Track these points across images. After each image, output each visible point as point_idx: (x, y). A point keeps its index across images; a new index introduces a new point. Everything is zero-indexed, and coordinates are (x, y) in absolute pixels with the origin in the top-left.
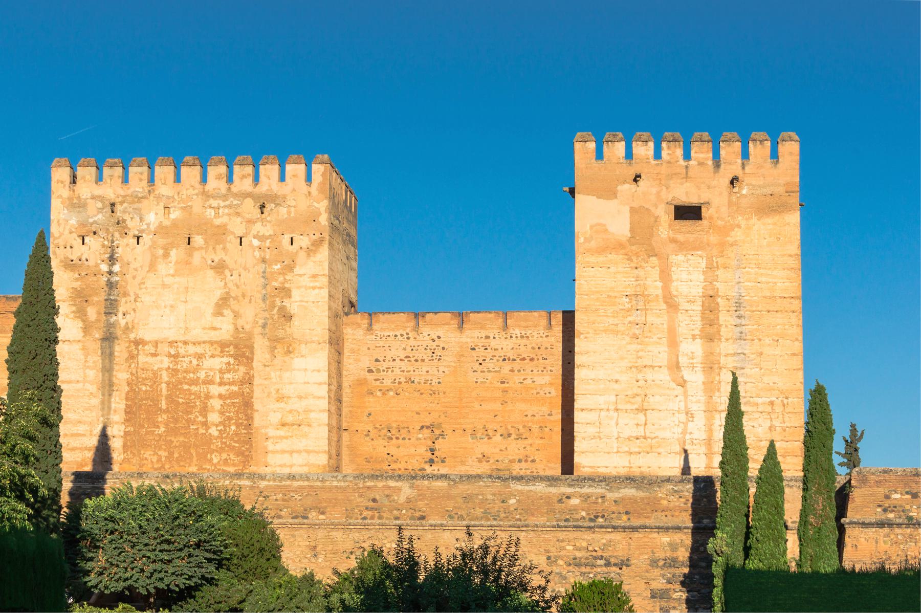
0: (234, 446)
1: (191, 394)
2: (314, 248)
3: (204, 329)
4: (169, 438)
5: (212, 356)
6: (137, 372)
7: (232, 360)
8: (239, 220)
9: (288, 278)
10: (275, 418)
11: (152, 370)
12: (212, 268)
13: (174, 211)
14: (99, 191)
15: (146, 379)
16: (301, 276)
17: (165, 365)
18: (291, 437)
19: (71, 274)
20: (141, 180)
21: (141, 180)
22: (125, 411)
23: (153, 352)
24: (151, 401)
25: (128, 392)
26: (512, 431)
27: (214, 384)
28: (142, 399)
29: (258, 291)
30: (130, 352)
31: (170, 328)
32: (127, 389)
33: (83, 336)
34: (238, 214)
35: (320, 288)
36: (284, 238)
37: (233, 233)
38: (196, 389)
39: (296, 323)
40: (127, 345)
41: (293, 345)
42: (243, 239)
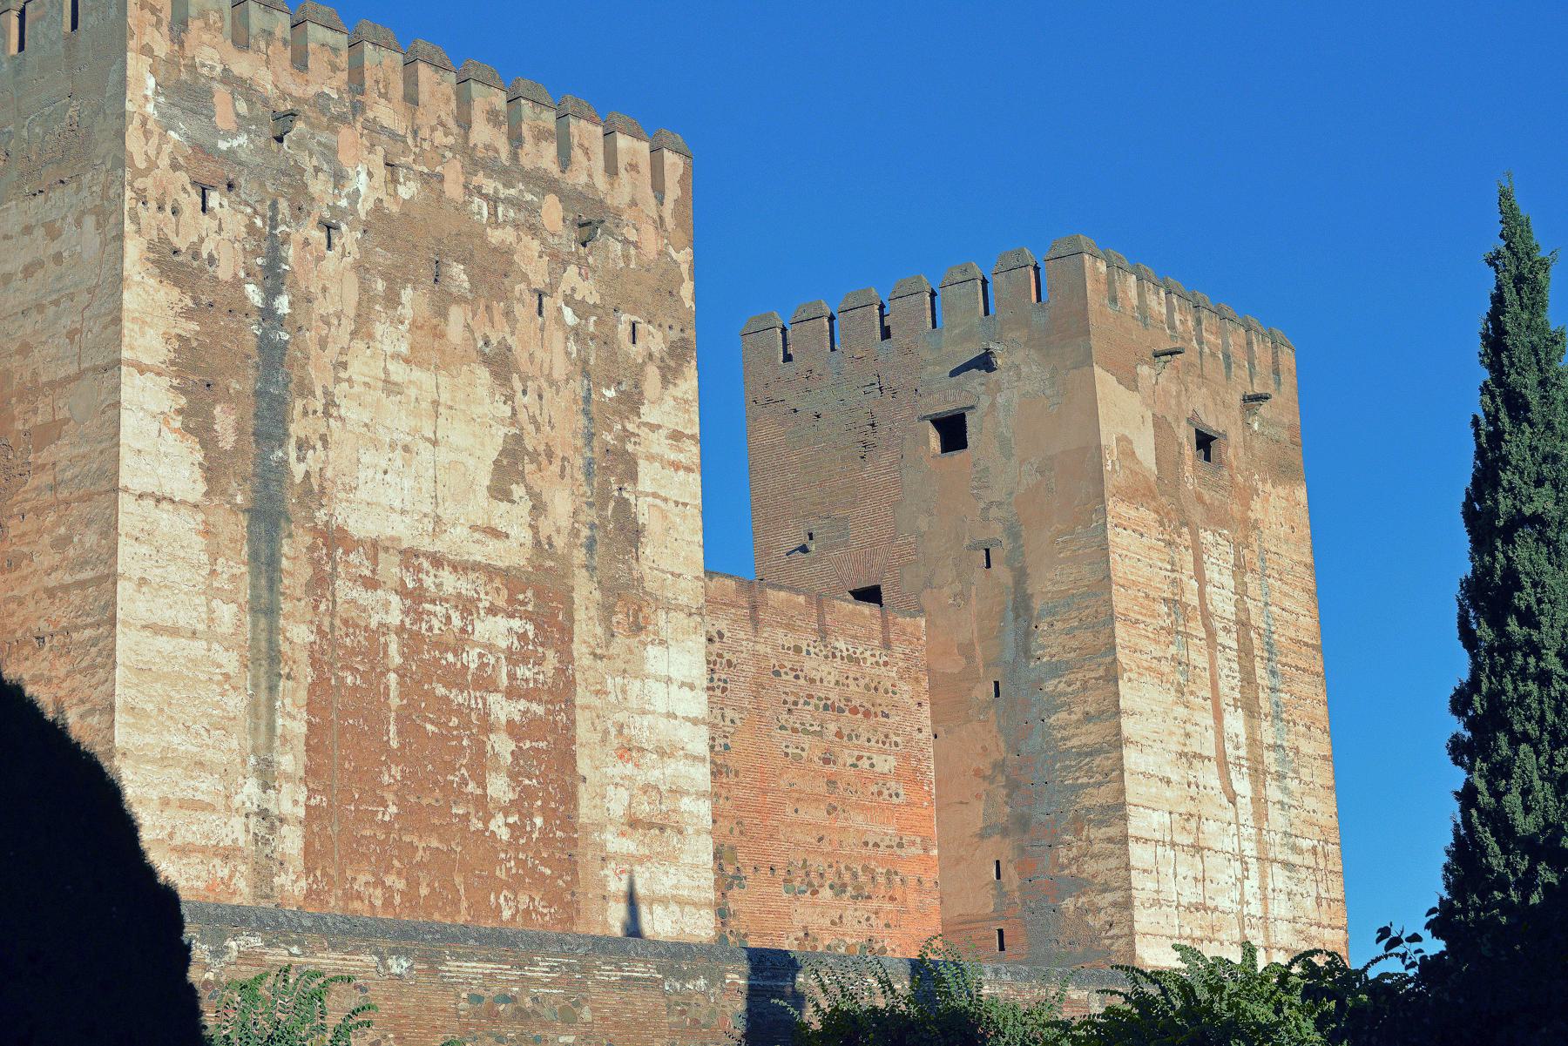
0: (542, 874)
1: (451, 712)
2: (672, 364)
3: (474, 528)
4: (407, 838)
5: (492, 611)
6: (332, 625)
7: (530, 628)
8: (536, 245)
9: (630, 427)
10: (618, 803)
11: (366, 629)
12: (487, 361)
13: (407, 179)
14: (242, 66)
15: (353, 652)
16: (654, 428)
17: (395, 618)
18: (649, 858)
19: (176, 292)
20: (335, 68)
21: (335, 68)
22: (307, 744)
23: (367, 573)
24: (366, 720)
25: (313, 684)
26: (847, 877)
27: (496, 691)
28: (343, 714)
29: (576, 449)
30: (316, 563)
31: (403, 512)
32: (306, 674)
33: (206, 494)
34: (534, 230)
35: (689, 470)
36: (619, 320)
37: (525, 277)
38: (460, 699)
39: (648, 551)
40: (308, 540)
41: (646, 611)
42: (545, 299)
